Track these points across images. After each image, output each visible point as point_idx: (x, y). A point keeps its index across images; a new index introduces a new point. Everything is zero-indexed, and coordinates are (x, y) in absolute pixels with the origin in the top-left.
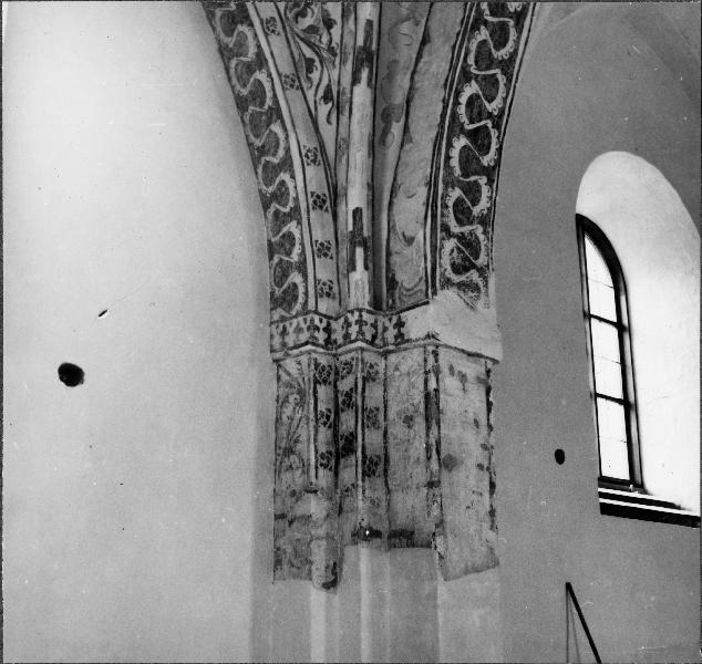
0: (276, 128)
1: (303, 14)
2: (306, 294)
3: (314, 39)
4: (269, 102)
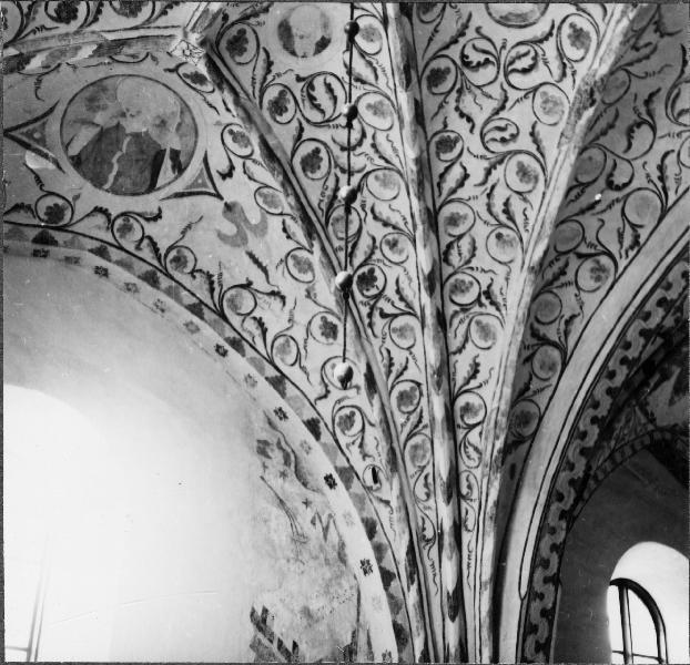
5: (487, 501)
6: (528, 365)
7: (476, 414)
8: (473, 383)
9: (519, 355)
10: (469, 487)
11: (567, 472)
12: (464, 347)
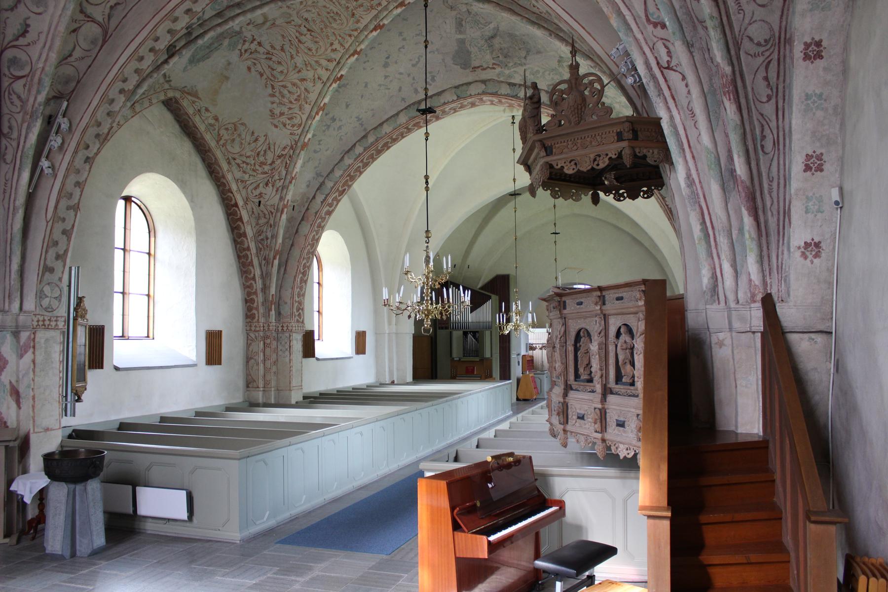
0: (251, 268)
1: (260, 235)
2: (259, 317)
3: (262, 242)
4: (249, 260)
5: (25, 142)
6: (74, 35)
7: (22, 68)
8: (22, 41)
9: (67, 28)
10: (10, 128)
11: (95, 128)
12: (16, 6)
